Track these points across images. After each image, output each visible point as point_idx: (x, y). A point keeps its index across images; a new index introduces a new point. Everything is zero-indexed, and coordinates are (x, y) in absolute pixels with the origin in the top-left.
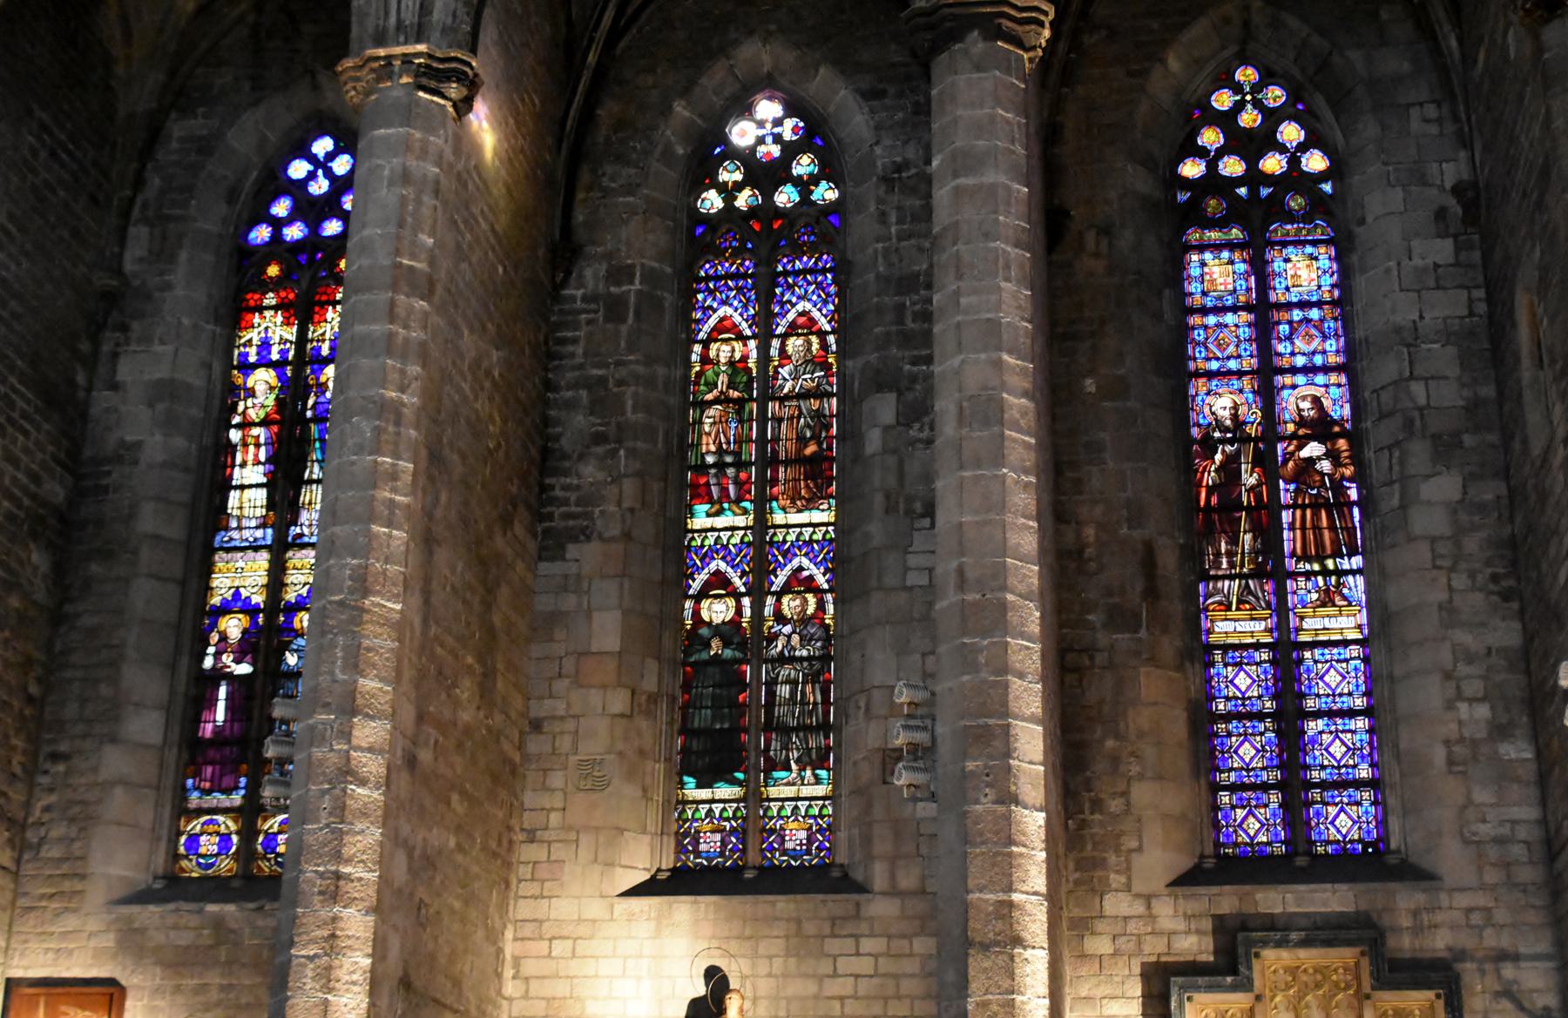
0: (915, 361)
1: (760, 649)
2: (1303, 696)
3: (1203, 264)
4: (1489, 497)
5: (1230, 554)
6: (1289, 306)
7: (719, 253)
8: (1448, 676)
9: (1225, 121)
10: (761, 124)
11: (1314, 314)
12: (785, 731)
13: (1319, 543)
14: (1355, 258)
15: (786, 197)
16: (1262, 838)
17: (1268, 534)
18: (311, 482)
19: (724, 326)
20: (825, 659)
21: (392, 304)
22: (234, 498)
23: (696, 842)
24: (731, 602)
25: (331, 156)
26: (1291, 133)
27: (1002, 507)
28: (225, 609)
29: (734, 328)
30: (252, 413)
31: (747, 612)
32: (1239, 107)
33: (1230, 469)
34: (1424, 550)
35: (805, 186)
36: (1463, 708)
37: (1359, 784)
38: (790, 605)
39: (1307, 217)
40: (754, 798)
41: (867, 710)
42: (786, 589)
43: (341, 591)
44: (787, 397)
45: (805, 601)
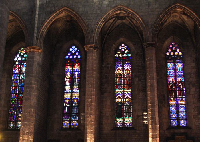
0: (140, 74)
1: (124, 104)
2: (179, 110)
3: (169, 64)
4: (198, 90)
5: (172, 95)
6: (178, 69)
7: (118, 61)
8: (193, 109)
9: (171, 49)
10: (122, 47)
11: (180, 70)
12: (127, 113)
13: (181, 94)
14: (184, 64)
15: (125, 55)
16: (175, 124)
17: (176, 93)
18: (75, 85)
19: (119, 69)
20: (131, 106)
21: (92, 73)
22: (66, 87)
23: (118, 124)
24: (121, 99)
25: (74, 48)
26: (178, 50)
27: (154, 96)
28: (66, 99)
29: (120, 70)
30: (68, 78)
31: (122, 100)
32: (172, 47)
33: (172, 86)
34: (191, 95)
35: (127, 54)
36: (195, 112)
37: (184, 119)
38: (127, 100)
39: (180, 59)
40: (124, 120)
41: (136, 111)
42: (126, 98)
43: (89, 102)
44: (126, 77)
45: (128, 100)
